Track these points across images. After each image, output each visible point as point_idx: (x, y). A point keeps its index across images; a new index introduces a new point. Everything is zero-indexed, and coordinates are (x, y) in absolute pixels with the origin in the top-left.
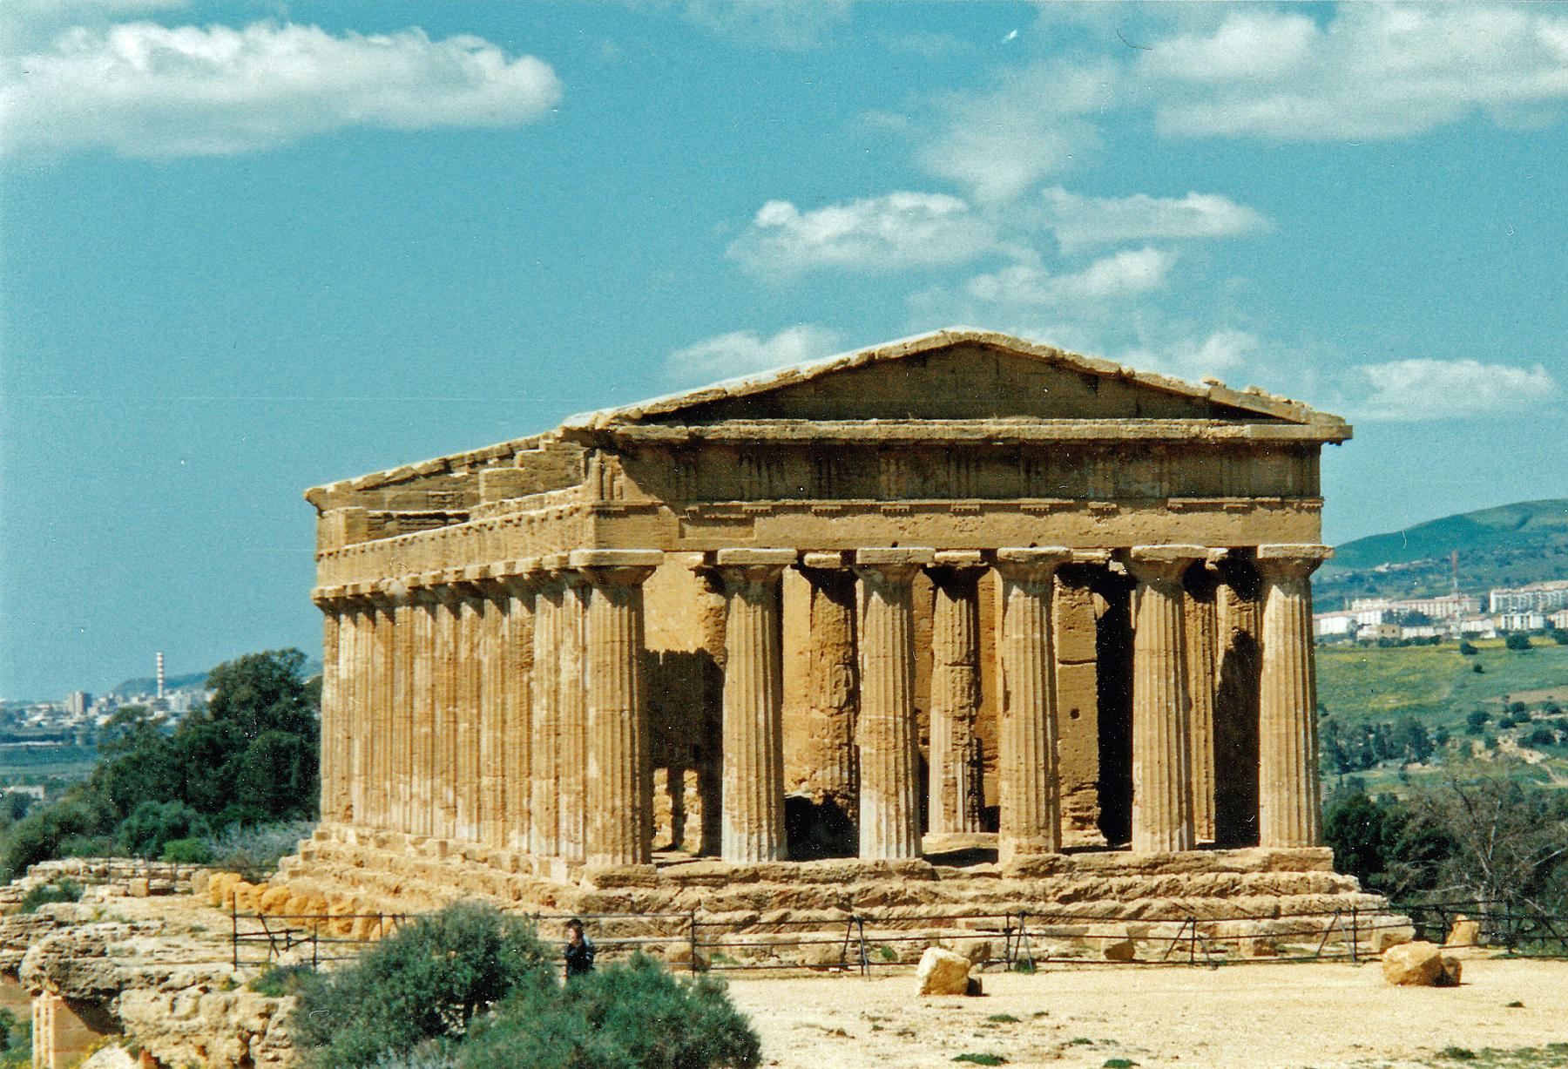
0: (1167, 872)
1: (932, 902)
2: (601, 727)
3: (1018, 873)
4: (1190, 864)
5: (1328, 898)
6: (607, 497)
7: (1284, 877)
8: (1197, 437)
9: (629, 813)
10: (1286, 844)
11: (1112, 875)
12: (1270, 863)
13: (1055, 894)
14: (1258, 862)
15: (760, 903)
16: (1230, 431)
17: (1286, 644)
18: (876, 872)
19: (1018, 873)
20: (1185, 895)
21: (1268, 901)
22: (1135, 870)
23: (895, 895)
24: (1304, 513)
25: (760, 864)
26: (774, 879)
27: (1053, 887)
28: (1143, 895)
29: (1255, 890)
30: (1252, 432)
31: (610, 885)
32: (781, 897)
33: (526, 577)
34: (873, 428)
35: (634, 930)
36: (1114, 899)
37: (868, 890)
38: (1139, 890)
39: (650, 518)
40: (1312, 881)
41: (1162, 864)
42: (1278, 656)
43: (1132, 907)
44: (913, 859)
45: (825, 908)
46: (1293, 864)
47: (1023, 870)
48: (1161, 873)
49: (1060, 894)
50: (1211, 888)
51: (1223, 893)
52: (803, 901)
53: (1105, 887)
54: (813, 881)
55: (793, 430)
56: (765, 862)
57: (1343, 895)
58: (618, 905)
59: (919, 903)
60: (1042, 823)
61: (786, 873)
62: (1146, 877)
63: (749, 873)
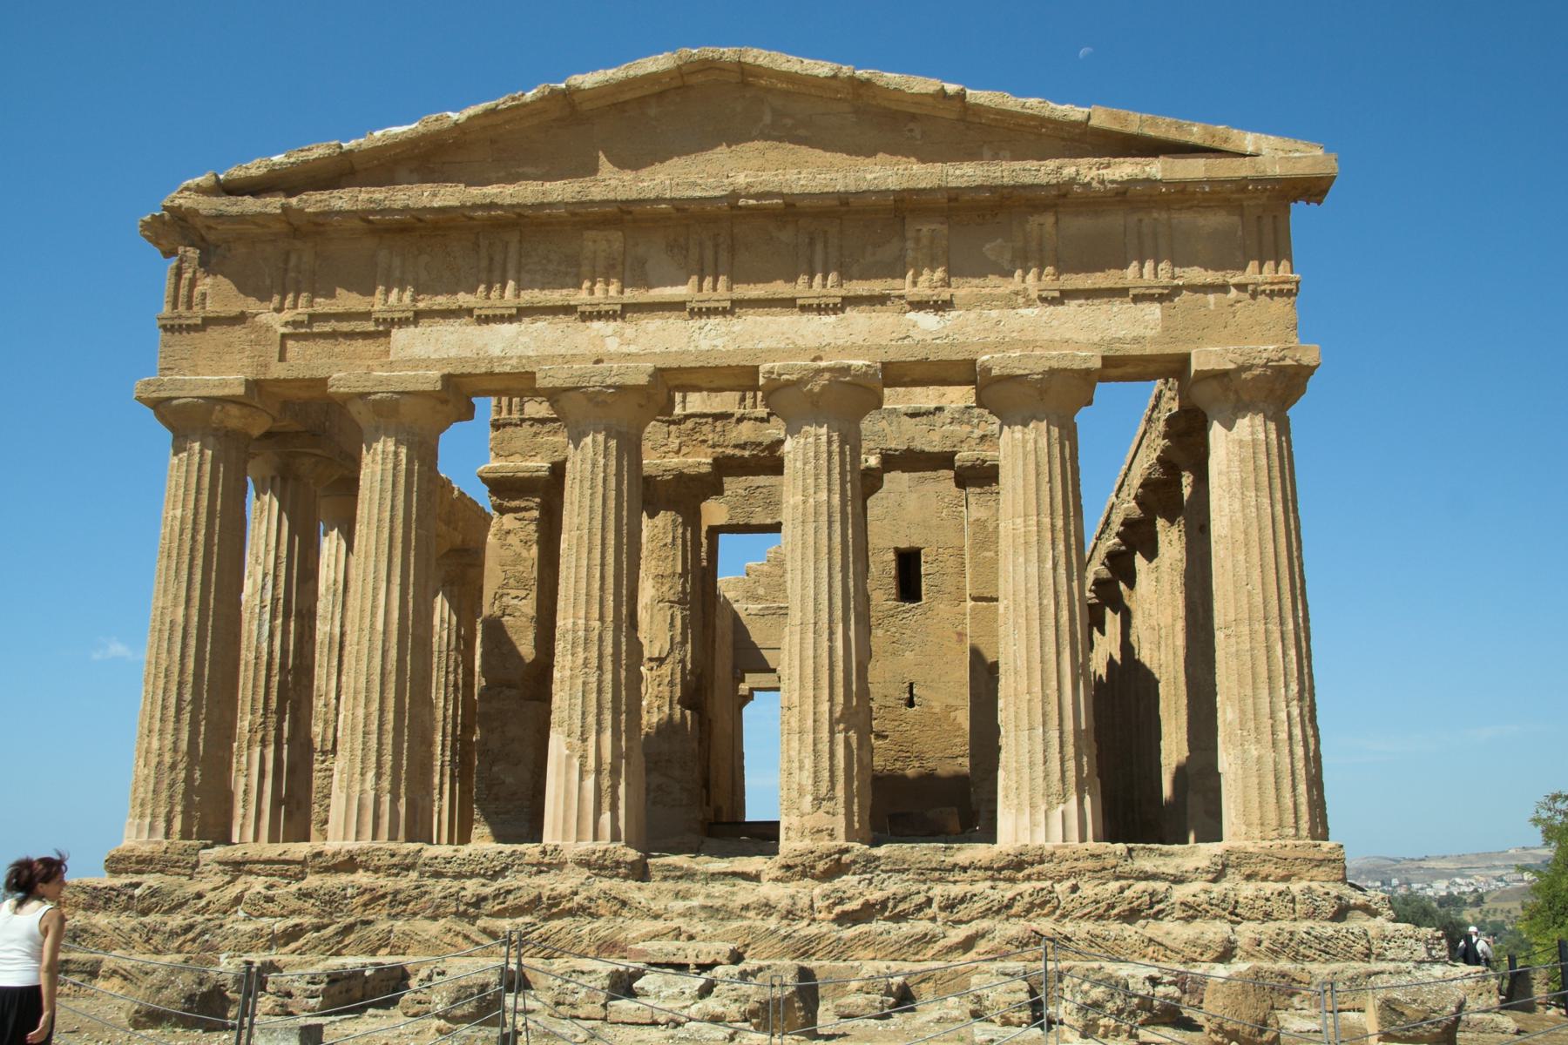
0: (1040, 876)
1: (616, 914)
3: (779, 873)
4: (1080, 864)
5: (1329, 929)
6: (182, 309)
7: (1248, 890)
8: (1072, 181)
9: (168, 759)
10: (1256, 833)
11: (940, 880)
12: (1225, 866)
13: (829, 909)
15: (332, 902)
16: (1125, 169)
17: (1244, 507)
18: (539, 864)
19: (779, 873)
20: (1064, 916)
21: (1215, 931)
22: (980, 874)
23: (555, 900)
24: (1261, 298)
26: (377, 870)
27: (826, 896)
28: (984, 915)
29: (1192, 912)
30: (1164, 170)
32: (366, 897)
33: (1192, 837)
34: (560, 191)
35: (106, 941)
36: (933, 919)
37: (509, 892)
38: (980, 905)
39: (238, 332)
40: (1299, 897)
41: (1032, 864)
42: (1233, 524)
43: (958, 934)
44: (605, 843)
46: (1268, 868)
47: (788, 867)
48: (1028, 878)
49: (838, 909)
50: (1112, 906)
51: (1131, 916)
52: (398, 903)
53: (921, 899)
55: (435, 195)
56: (366, 843)
57: (1357, 923)
58: (108, 900)
59: (595, 916)
60: (823, 790)
61: (395, 860)
62: (1001, 884)
63: (340, 859)
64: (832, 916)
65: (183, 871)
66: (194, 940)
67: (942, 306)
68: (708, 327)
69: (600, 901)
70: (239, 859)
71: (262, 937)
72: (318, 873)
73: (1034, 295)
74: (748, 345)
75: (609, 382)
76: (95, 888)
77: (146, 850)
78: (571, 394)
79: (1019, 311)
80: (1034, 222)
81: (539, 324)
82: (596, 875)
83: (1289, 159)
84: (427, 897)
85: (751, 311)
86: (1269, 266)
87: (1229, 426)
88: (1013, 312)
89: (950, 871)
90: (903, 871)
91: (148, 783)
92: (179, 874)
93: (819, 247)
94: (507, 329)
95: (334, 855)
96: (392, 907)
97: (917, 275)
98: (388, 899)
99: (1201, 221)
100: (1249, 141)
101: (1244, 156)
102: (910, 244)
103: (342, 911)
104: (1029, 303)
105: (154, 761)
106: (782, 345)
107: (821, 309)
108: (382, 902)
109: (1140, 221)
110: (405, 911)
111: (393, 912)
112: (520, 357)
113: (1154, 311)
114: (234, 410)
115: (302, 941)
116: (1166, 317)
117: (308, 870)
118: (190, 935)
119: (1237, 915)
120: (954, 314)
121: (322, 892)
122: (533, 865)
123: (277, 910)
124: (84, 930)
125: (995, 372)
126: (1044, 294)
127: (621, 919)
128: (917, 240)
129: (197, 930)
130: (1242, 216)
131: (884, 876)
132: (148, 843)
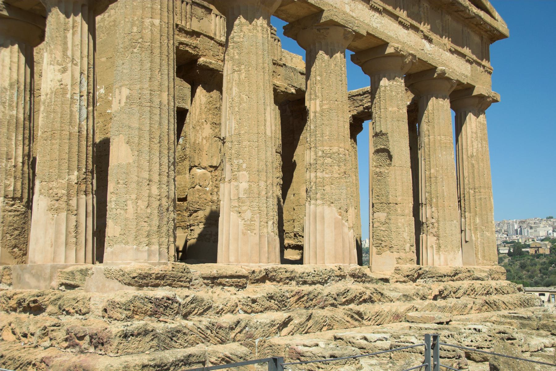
0: (460, 279)
1: (380, 300)
2: (136, 108)
14: (486, 274)
18: (340, 276)
20: (477, 294)
25: (270, 266)
31: (147, 285)
32: (296, 297)
45: (323, 308)
48: (457, 280)
54: (305, 283)
58: (166, 307)
61: (288, 275)
64: (432, 297)
65: (184, 284)
66: (240, 332)
67: (430, 41)
68: (375, 17)
69: (374, 294)
70: (216, 275)
71: (274, 325)
72: (253, 283)
73: (449, 47)
74: (386, 31)
75: (355, 28)
76: (157, 299)
77: (158, 269)
78: (340, 28)
82: (356, 281)
84: (320, 297)
85: (386, 16)
86: (487, 61)
87: (477, 116)
89: (442, 277)
90: (432, 277)
91: (152, 220)
92: (182, 286)
95: (260, 272)
96: (307, 302)
97: (424, 25)
98: (305, 298)
100: (496, 15)
102: (421, 9)
103: (286, 306)
105: (156, 204)
106: (395, 37)
108: (302, 299)
110: (311, 305)
111: (307, 305)
115: (290, 327)
116: (472, 70)
117: (248, 282)
118: (238, 329)
120: (432, 46)
121: (278, 295)
122: (337, 276)
123: (259, 308)
124: (179, 331)
125: (447, 75)
126: (452, 49)
127: (380, 303)
128: (424, 9)
129: (243, 324)
130: (482, 40)
131: (429, 279)
132: (160, 264)
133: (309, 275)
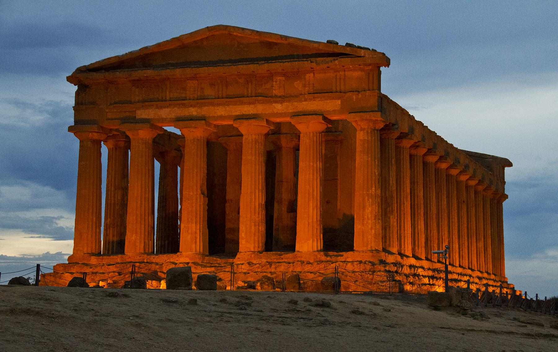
68: (219, 109)
79: (303, 103)
80: (308, 75)
81: (175, 108)
83: (373, 57)
88: (301, 103)
93: (250, 84)
94: (167, 110)
99: (354, 74)
101: (361, 57)
102: (274, 83)
104: (305, 100)
106: (239, 114)
107: (250, 103)
109: (336, 75)
112: (170, 118)
113: (339, 102)
114: (95, 134)
119: (346, 270)
120: (285, 104)
128: (276, 82)
133: (154, 258)
